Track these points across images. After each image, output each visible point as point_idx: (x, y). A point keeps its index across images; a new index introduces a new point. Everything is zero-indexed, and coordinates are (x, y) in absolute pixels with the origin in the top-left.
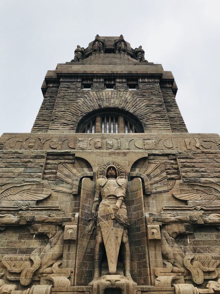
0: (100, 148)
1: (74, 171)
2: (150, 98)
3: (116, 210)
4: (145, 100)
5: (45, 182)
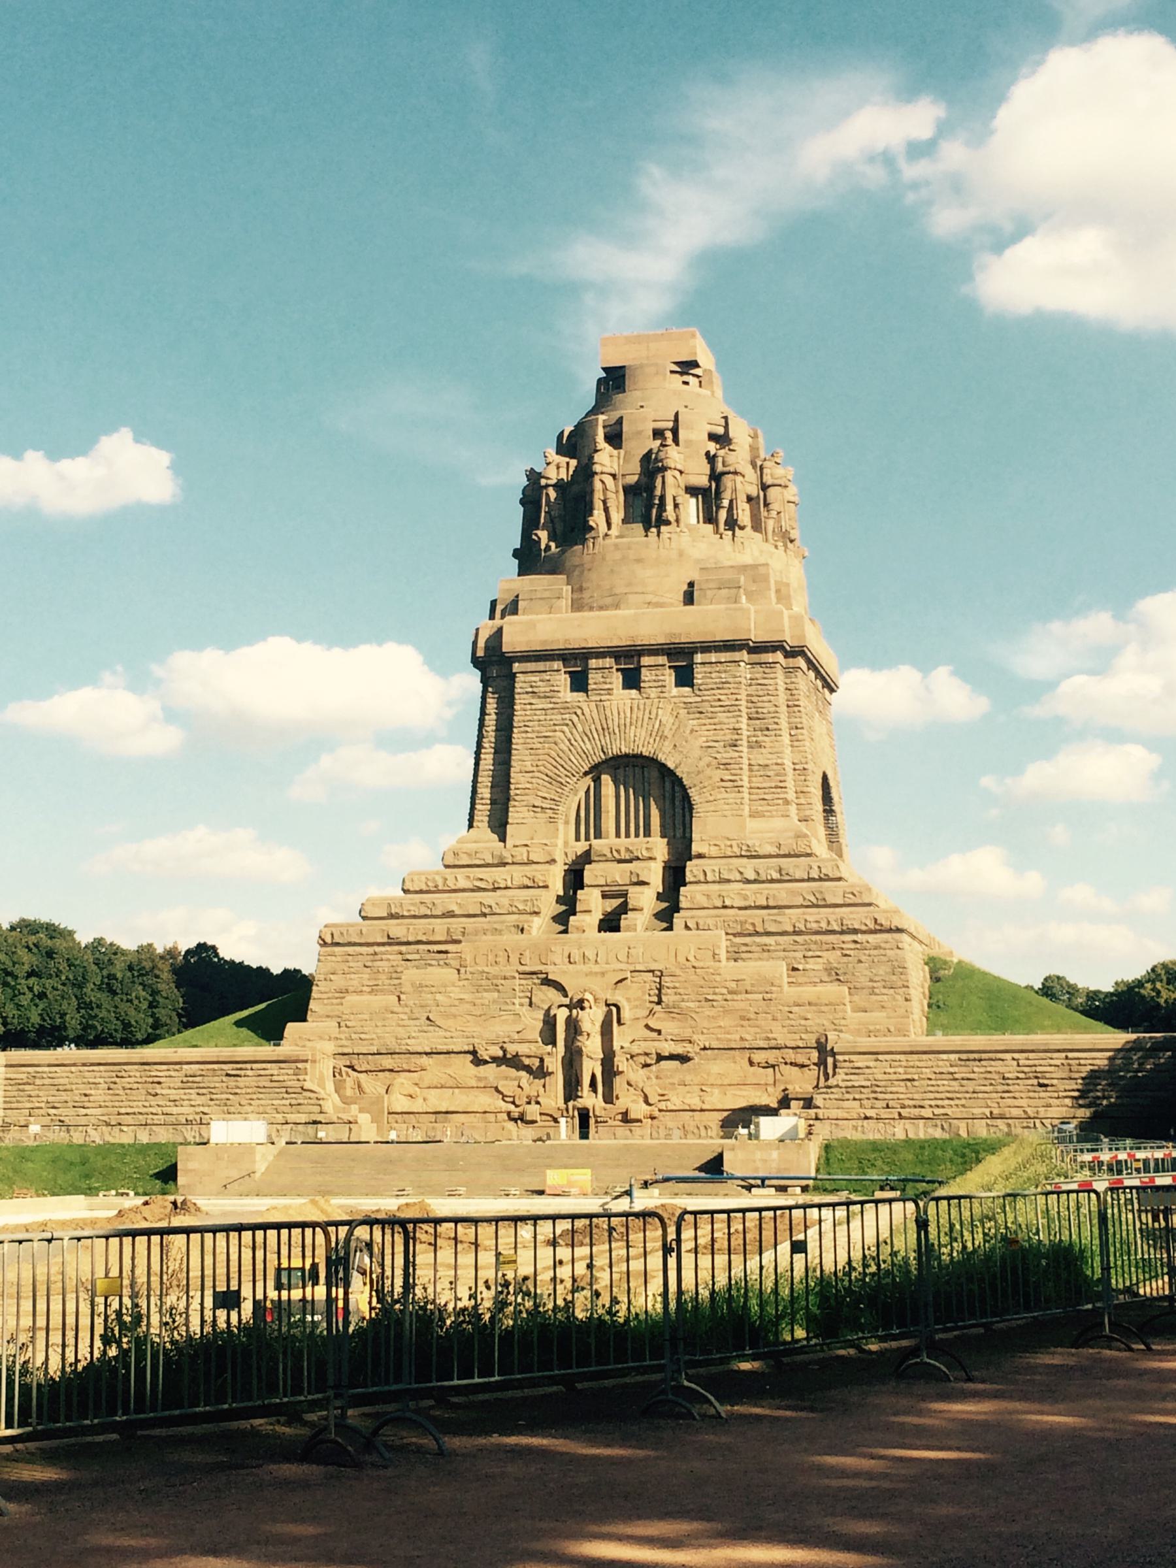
2: (716, 720)
4: (704, 728)
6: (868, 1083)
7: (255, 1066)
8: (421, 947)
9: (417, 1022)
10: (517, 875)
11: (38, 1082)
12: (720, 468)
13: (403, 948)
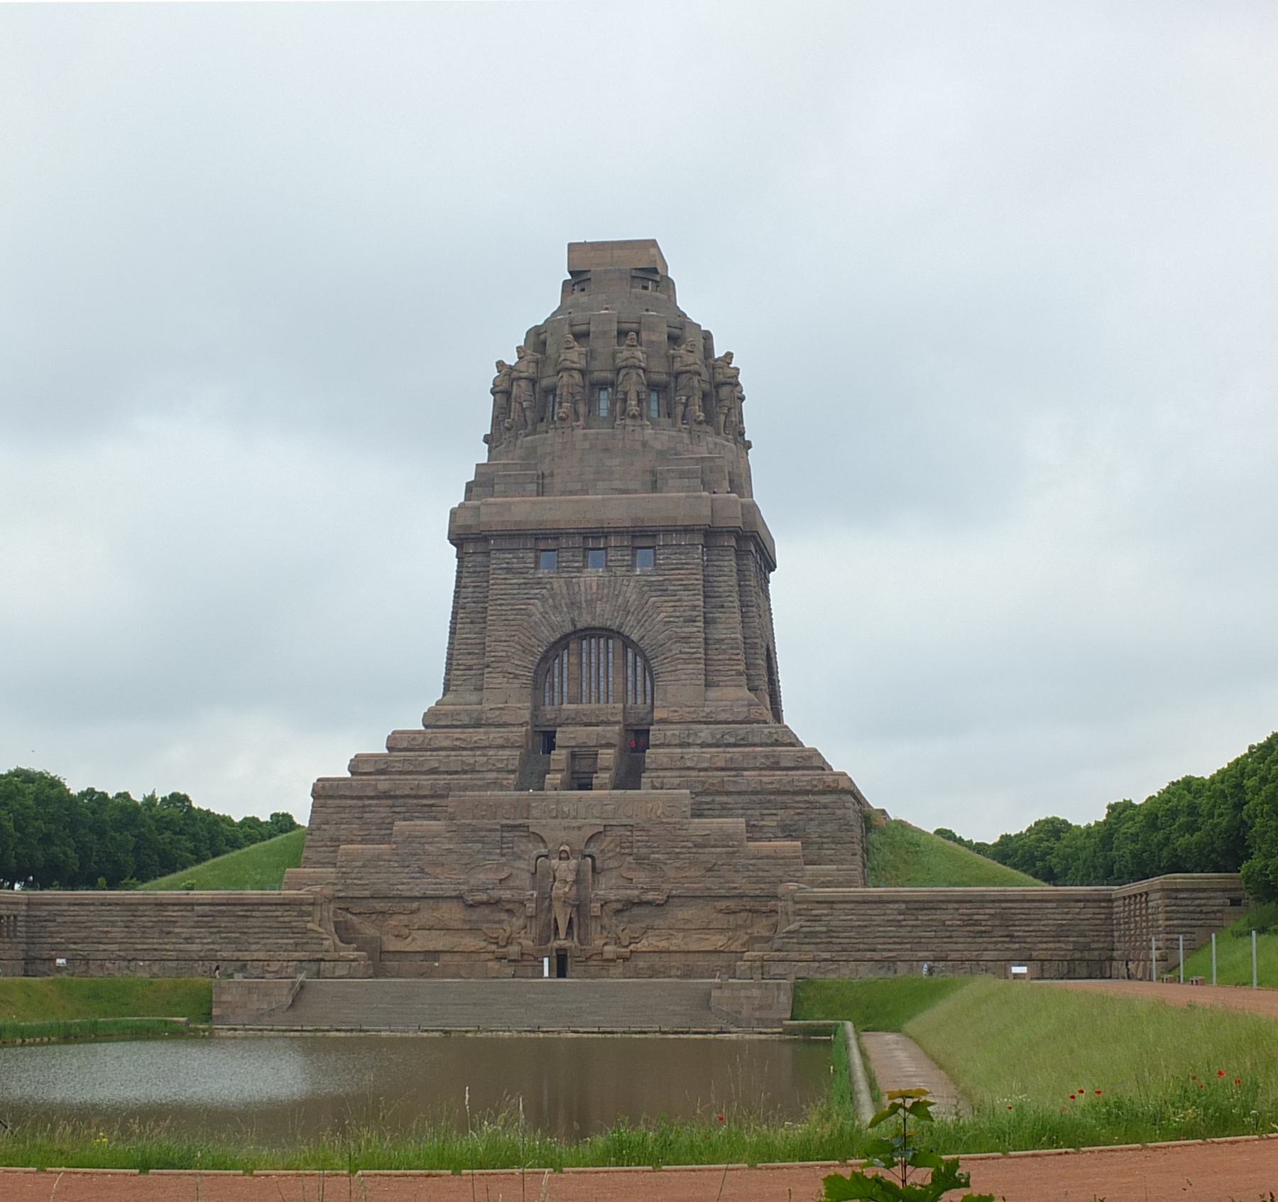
0: (555, 818)
1: (530, 846)
3: (565, 893)
5: (504, 860)
6: (824, 929)
7: (262, 908)
8: (408, 800)
9: (406, 870)
10: (496, 735)
11: (59, 919)
12: (678, 366)
13: (390, 802)
